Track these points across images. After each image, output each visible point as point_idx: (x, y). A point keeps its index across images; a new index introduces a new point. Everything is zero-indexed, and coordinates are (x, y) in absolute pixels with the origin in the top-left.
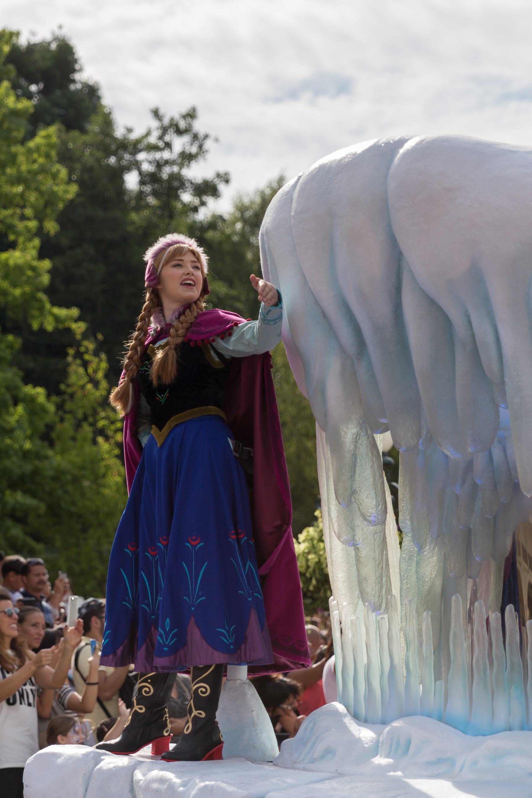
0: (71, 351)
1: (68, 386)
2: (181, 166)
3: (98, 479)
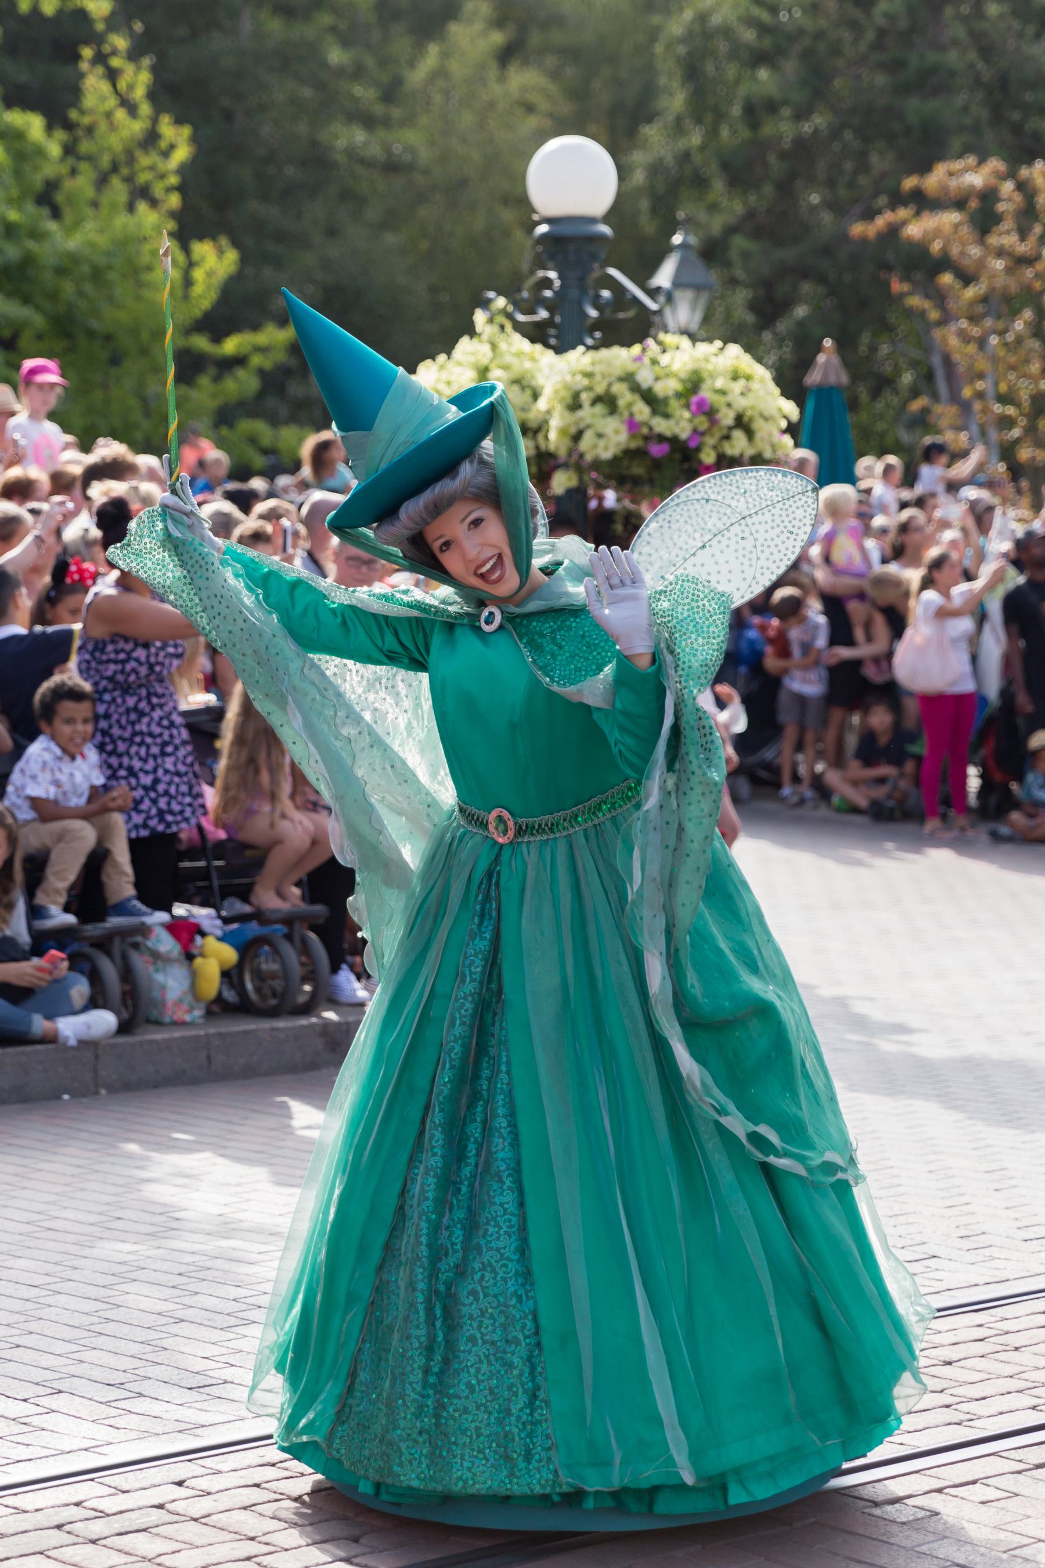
0: (87, 52)
1: (82, 112)
3: (137, 274)
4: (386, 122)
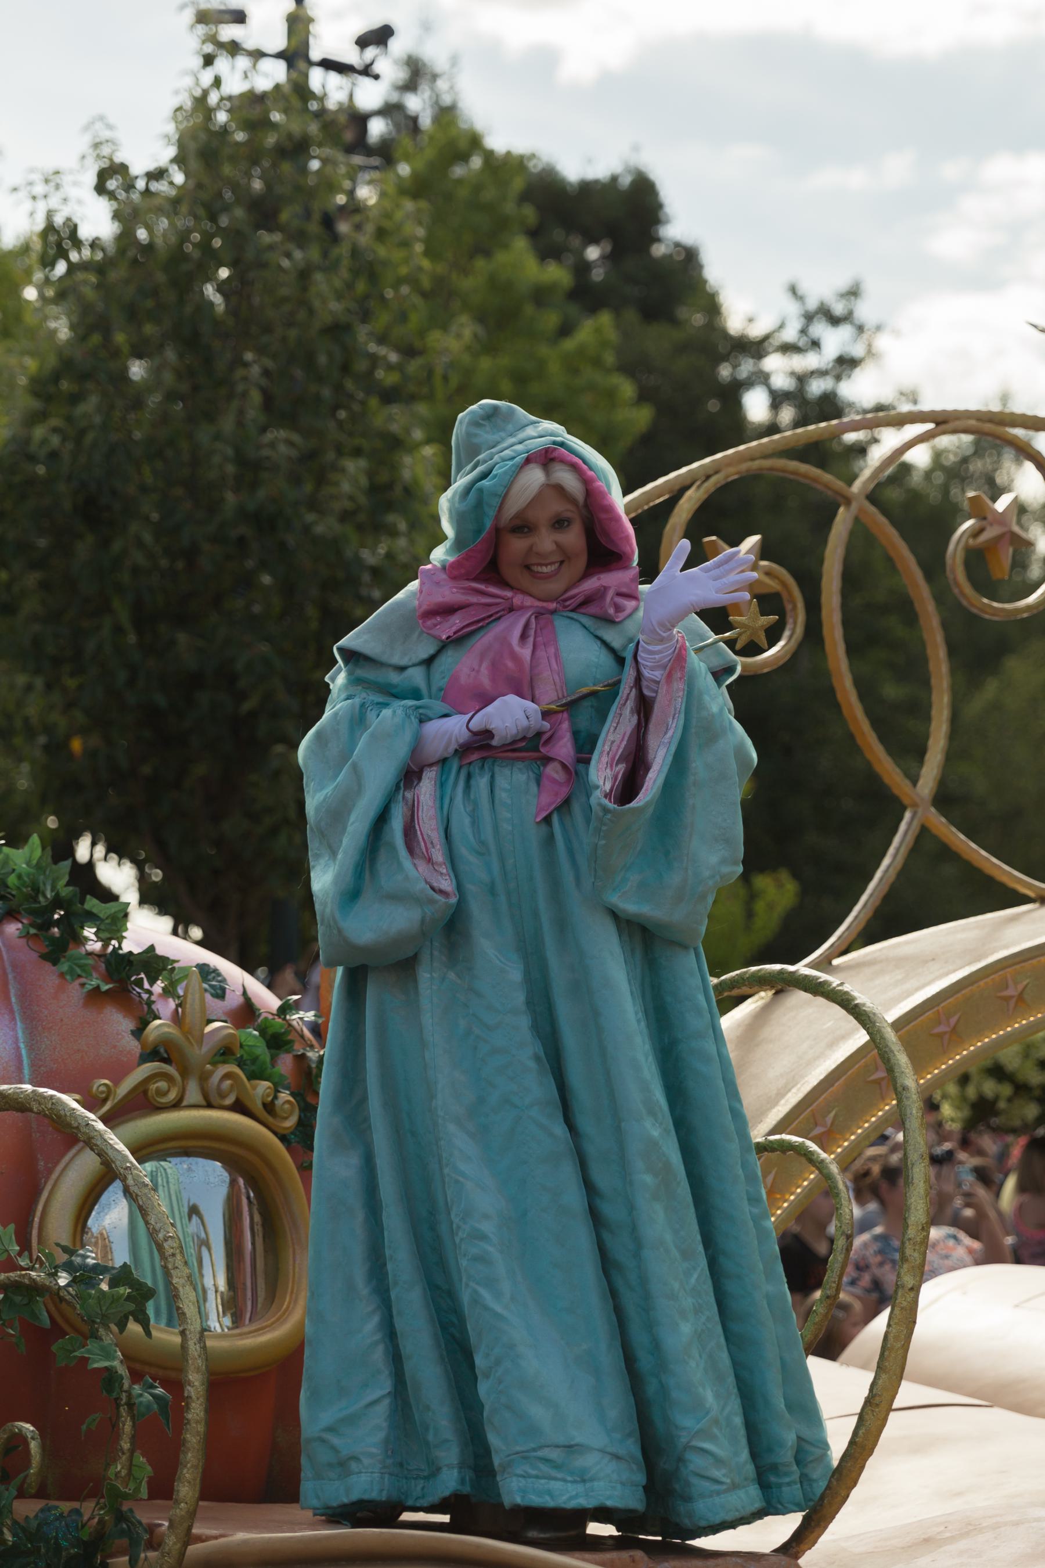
2: (838, 378)
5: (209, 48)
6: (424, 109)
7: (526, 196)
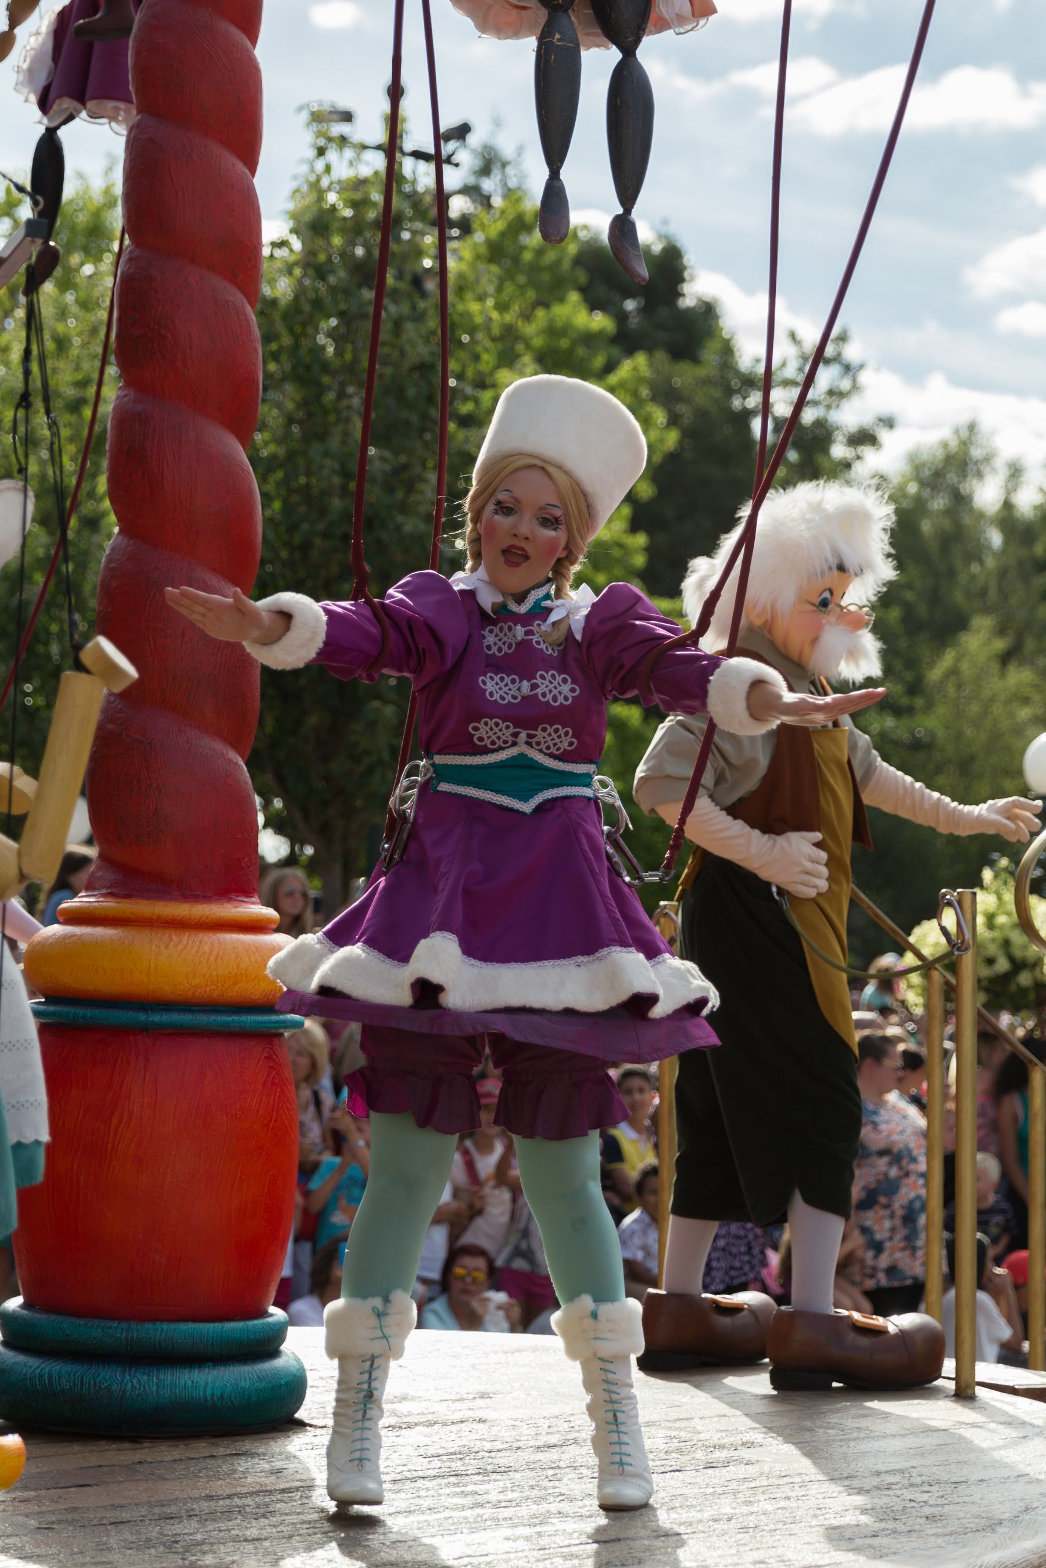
2: (828, 407)
4: (910, 711)
5: (322, 142)
6: (496, 190)
7: (579, 261)
